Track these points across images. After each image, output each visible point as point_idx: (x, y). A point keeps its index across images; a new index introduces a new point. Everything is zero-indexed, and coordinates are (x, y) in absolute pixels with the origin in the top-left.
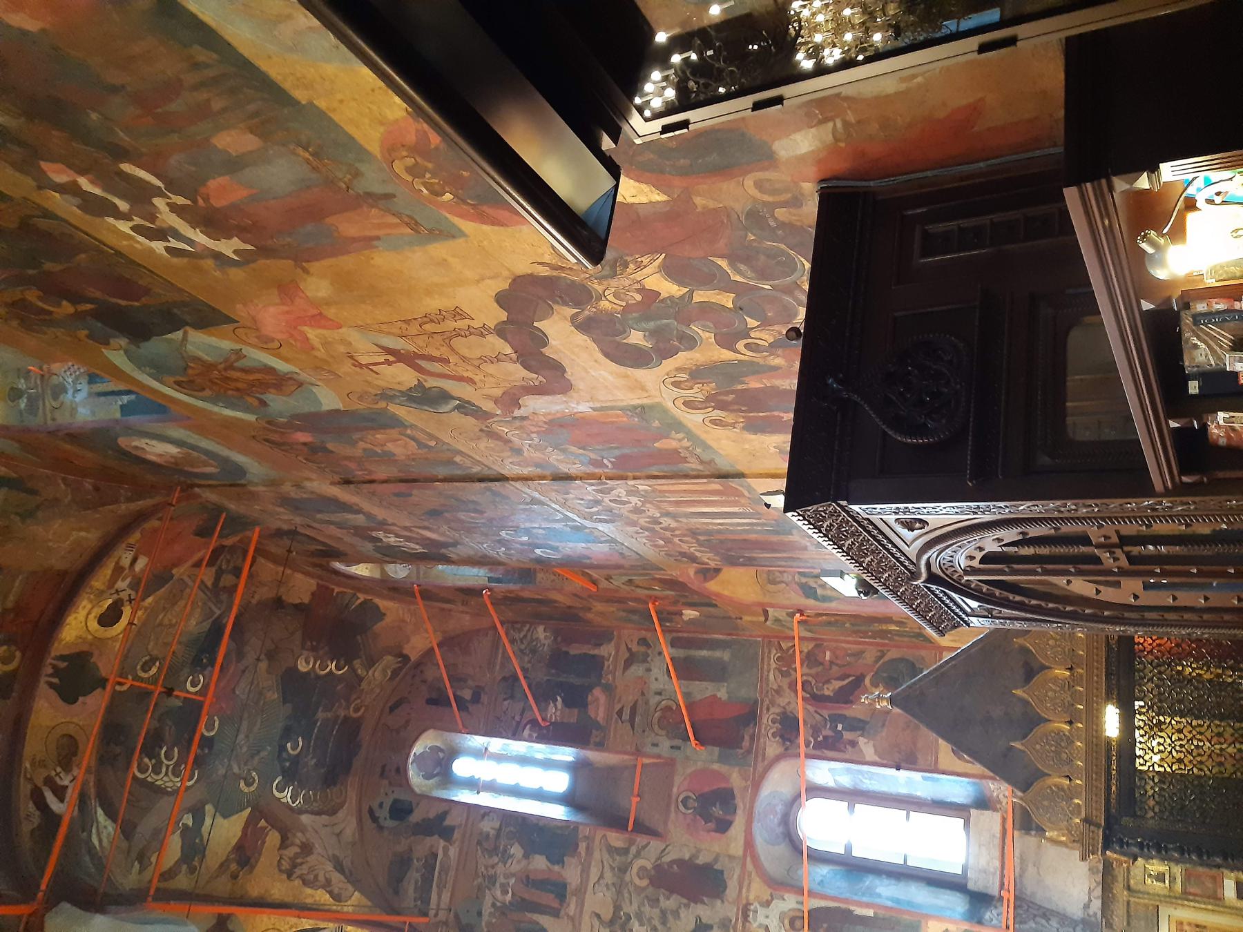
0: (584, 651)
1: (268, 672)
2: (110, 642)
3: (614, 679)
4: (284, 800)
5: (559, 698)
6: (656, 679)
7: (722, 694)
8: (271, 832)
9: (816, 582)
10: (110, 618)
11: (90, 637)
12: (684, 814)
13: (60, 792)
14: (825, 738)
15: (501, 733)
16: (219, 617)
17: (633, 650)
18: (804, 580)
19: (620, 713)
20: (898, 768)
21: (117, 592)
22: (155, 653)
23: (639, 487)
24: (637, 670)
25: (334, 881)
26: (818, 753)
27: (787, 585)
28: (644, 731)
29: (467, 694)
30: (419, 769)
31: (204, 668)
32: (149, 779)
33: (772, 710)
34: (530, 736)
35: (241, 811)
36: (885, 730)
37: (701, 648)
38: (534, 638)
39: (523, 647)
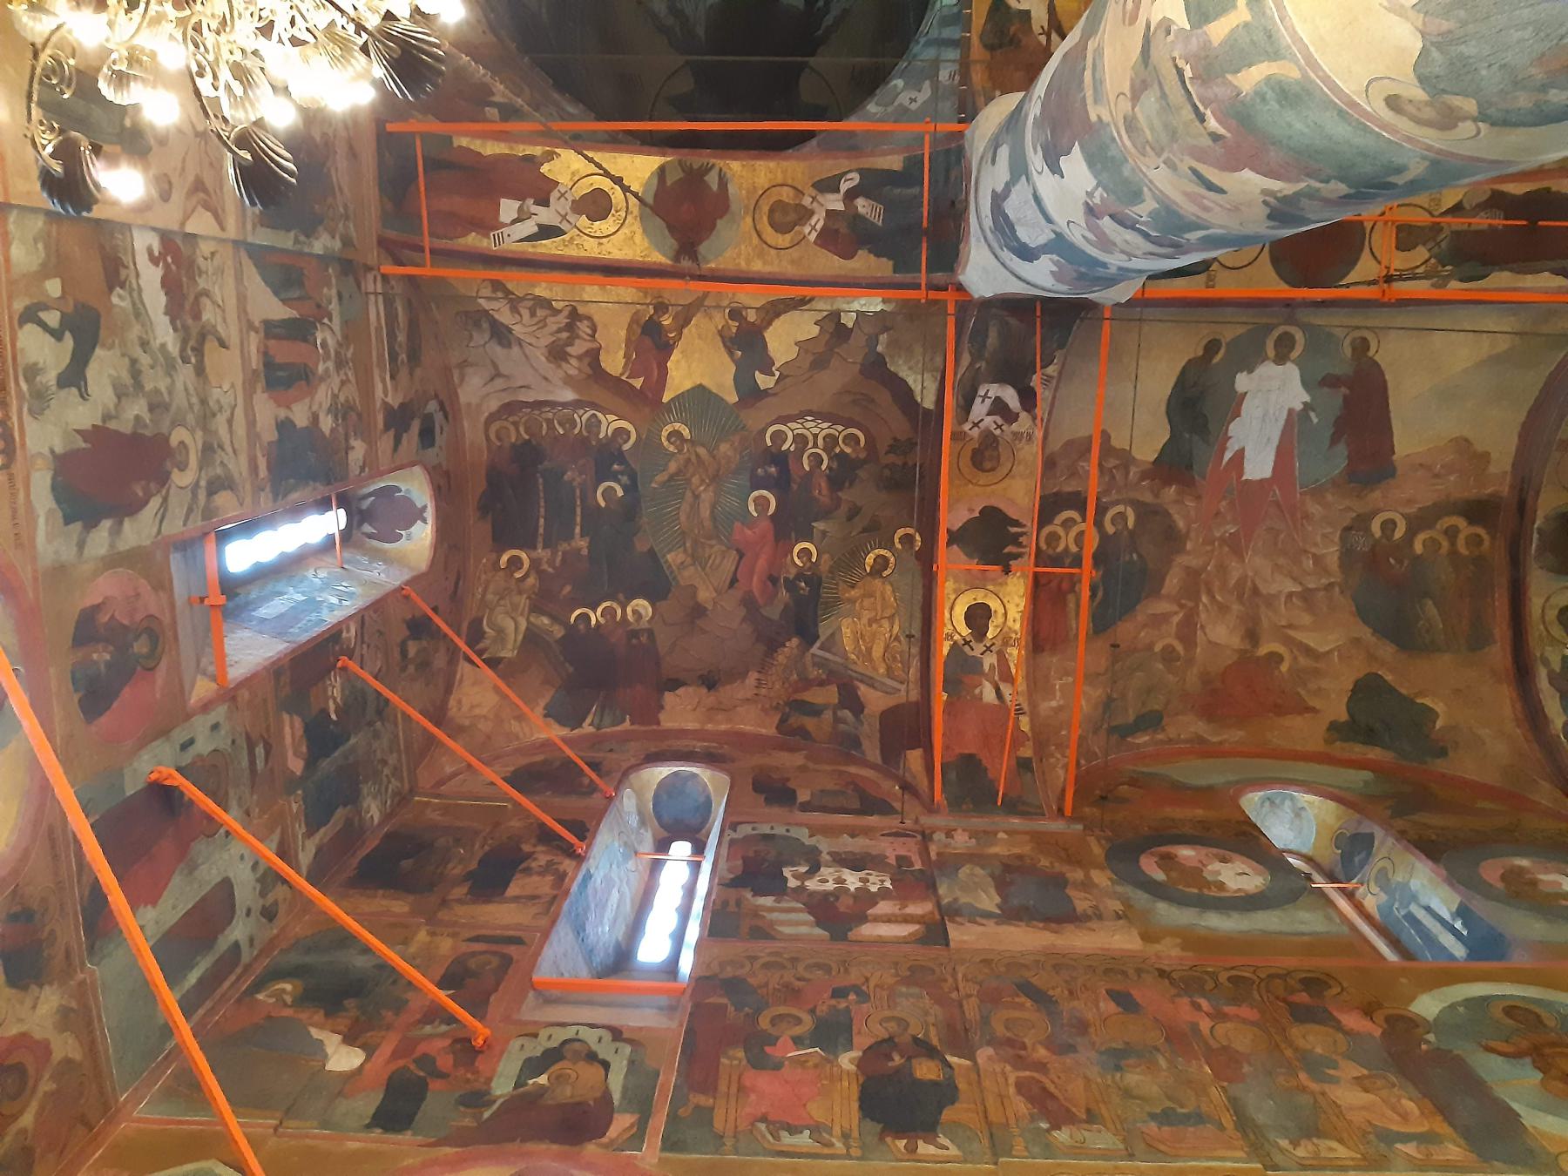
1: (693, 590)
2: (963, 587)
4: (611, 417)
5: (334, 717)
8: (620, 370)
10: (978, 617)
11: (991, 588)
13: (999, 407)
16: (811, 644)
21: (988, 649)
22: (878, 582)
25: (506, 310)
28: (233, 742)
30: (408, 501)
31: (800, 575)
32: (840, 428)
35: (678, 396)
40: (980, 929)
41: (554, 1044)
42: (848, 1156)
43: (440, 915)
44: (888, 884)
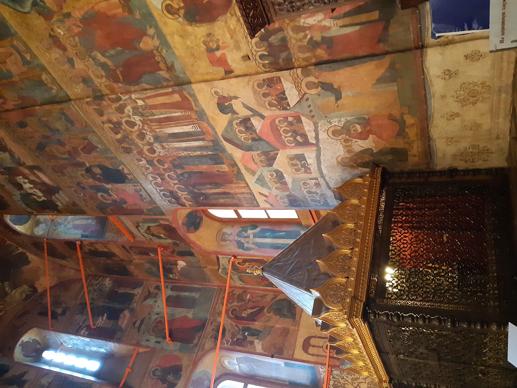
0: (126, 291)
3: (137, 305)
5: (106, 315)
6: (158, 306)
7: (190, 314)
9: (245, 240)
12: (152, 378)
14: (238, 339)
15: (71, 332)
17: (151, 291)
18: (239, 239)
19: (134, 323)
20: (272, 357)
23: (138, 101)
24: (150, 302)
26: (232, 347)
27: (230, 242)
28: (144, 333)
29: (59, 311)
30: (22, 350)
33: (213, 324)
34: (84, 333)
36: (270, 336)
37: (186, 291)
38: (103, 283)
39: (96, 288)
40: (21, 158)
41: (150, 236)
42: (141, 185)
43: (127, 259)
44: (21, 177)
